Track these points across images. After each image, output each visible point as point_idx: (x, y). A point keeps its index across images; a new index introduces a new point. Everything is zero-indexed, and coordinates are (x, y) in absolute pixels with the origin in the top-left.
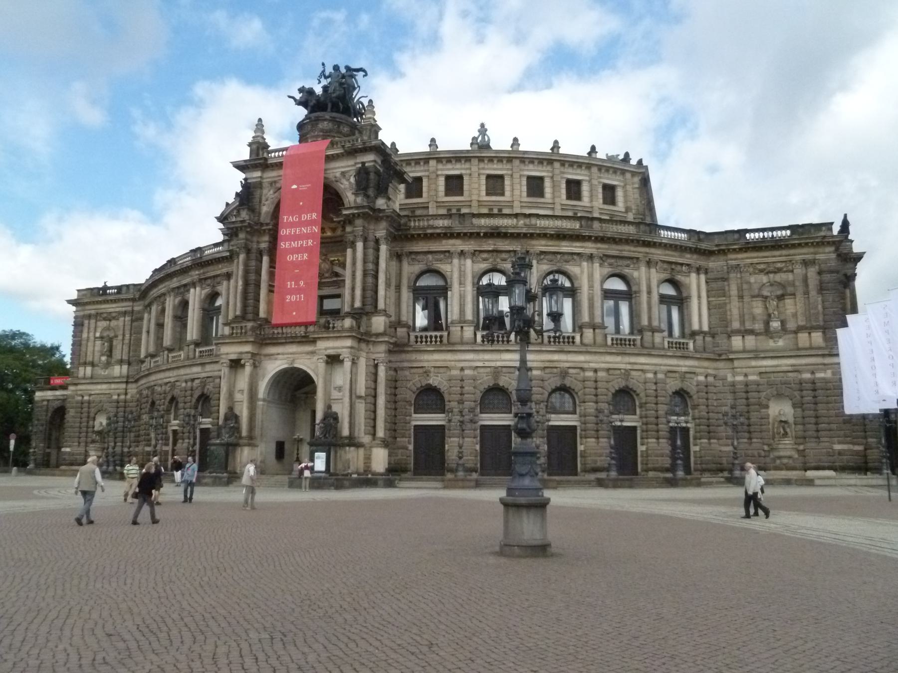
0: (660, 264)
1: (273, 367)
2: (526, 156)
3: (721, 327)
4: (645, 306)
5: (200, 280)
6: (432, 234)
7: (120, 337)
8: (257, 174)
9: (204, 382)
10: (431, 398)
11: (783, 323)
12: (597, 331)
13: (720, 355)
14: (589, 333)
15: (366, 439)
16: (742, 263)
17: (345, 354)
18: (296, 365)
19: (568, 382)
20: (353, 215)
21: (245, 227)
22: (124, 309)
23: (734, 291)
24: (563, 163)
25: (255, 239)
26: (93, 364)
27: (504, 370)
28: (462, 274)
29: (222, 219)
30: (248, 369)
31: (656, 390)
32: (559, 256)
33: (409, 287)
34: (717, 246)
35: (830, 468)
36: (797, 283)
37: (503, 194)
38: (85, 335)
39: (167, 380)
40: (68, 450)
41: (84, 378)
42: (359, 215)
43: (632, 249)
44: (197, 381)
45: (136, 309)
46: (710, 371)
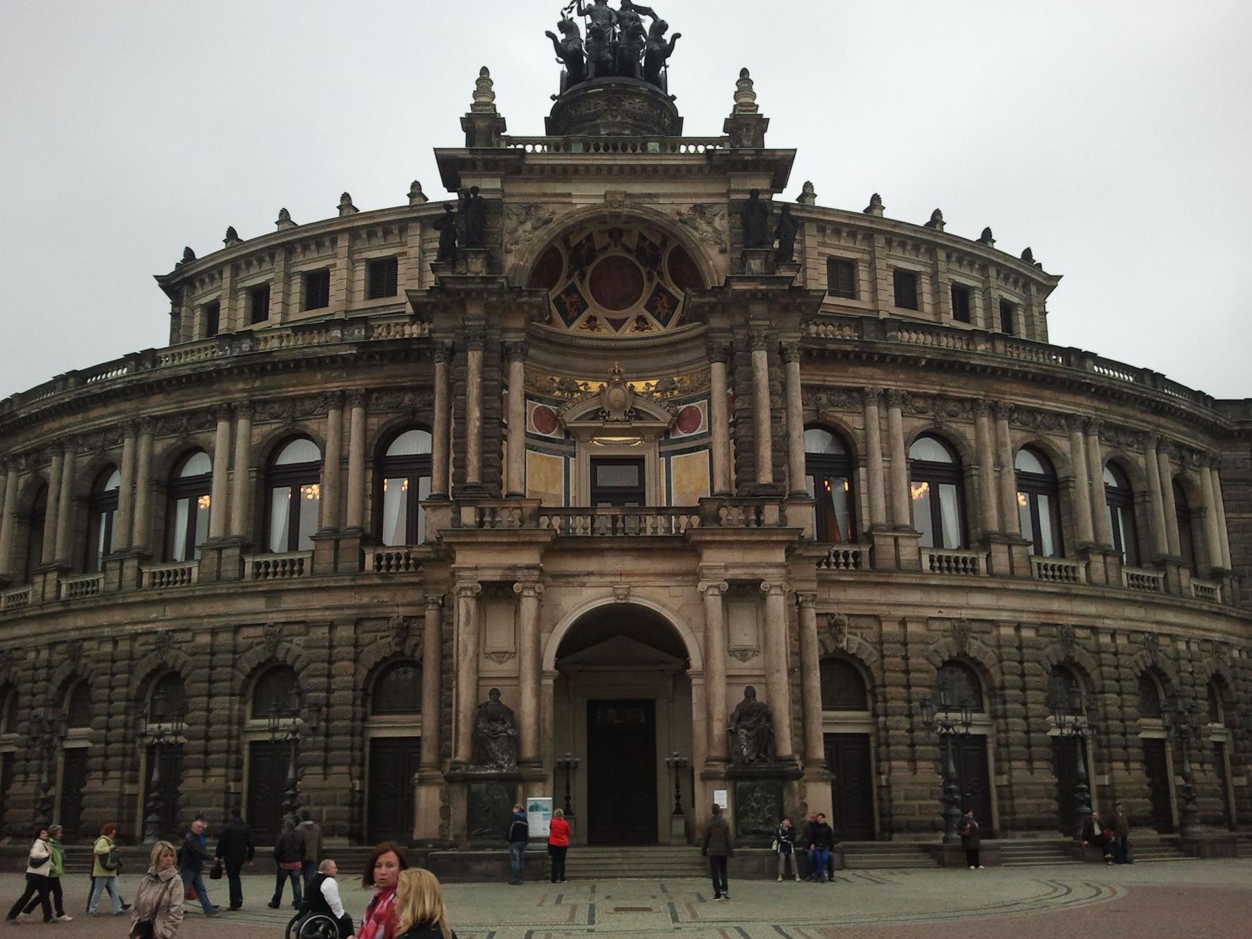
1: (578, 602)
6: (834, 353)
8: (496, 184)
9: (275, 635)
10: (847, 677)
12: (1109, 559)
14: (1097, 562)
15: (799, 763)
17: (773, 578)
18: (632, 600)
19: (1078, 653)
21: (491, 292)
25: (494, 320)
27: (975, 626)
28: (887, 434)
29: (179, 284)
30: (529, 606)
31: (1191, 673)
32: (1039, 418)
34: (1240, 423)
37: (853, 295)
39: (139, 628)
42: (765, 294)
43: (1139, 415)
44: (247, 632)
46: (1243, 642)
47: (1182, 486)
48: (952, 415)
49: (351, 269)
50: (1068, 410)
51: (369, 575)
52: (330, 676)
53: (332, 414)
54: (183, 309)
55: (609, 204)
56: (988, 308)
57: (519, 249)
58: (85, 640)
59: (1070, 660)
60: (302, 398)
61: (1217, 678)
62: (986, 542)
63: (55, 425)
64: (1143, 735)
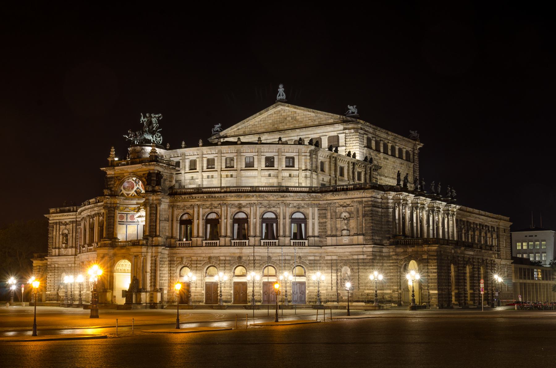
0: (291, 206)
3: (324, 234)
4: (281, 226)
5: (98, 213)
7: (71, 235)
22: (72, 220)
23: (329, 217)
26: (59, 248)
33: (177, 221)
35: (362, 301)
36: (355, 213)
38: (54, 233)
40: (49, 293)
41: (55, 256)
45: (78, 219)
46: (316, 254)
50: (248, 202)
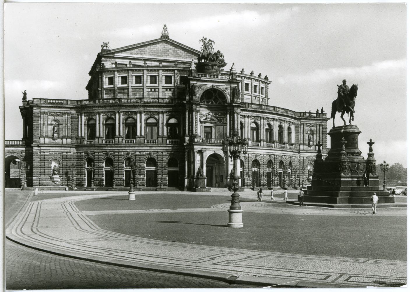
2: (247, 76)
3: (298, 143)
5: (145, 111)
11: (313, 142)
13: (297, 151)
16: (304, 123)
18: (217, 153)
20: (236, 105)
23: (302, 131)
24: (254, 79)
26: (47, 137)
27: (258, 155)
30: (204, 154)
34: (299, 117)
36: (317, 131)
39: (124, 150)
44: (146, 152)
45: (72, 112)
46: (295, 156)
47: (289, 128)
48: (257, 119)
49: (147, 77)
51: (168, 144)
52: (162, 160)
53: (161, 115)
54: (104, 78)
55: (213, 87)
56: (259, 89)
57: (199, 94)
58: (110, 151)
59: (270, 160)
60: (153, 112)
61: (290, 163)
62: (260, 141)
63: (97, 108)
64: (280, 171)
